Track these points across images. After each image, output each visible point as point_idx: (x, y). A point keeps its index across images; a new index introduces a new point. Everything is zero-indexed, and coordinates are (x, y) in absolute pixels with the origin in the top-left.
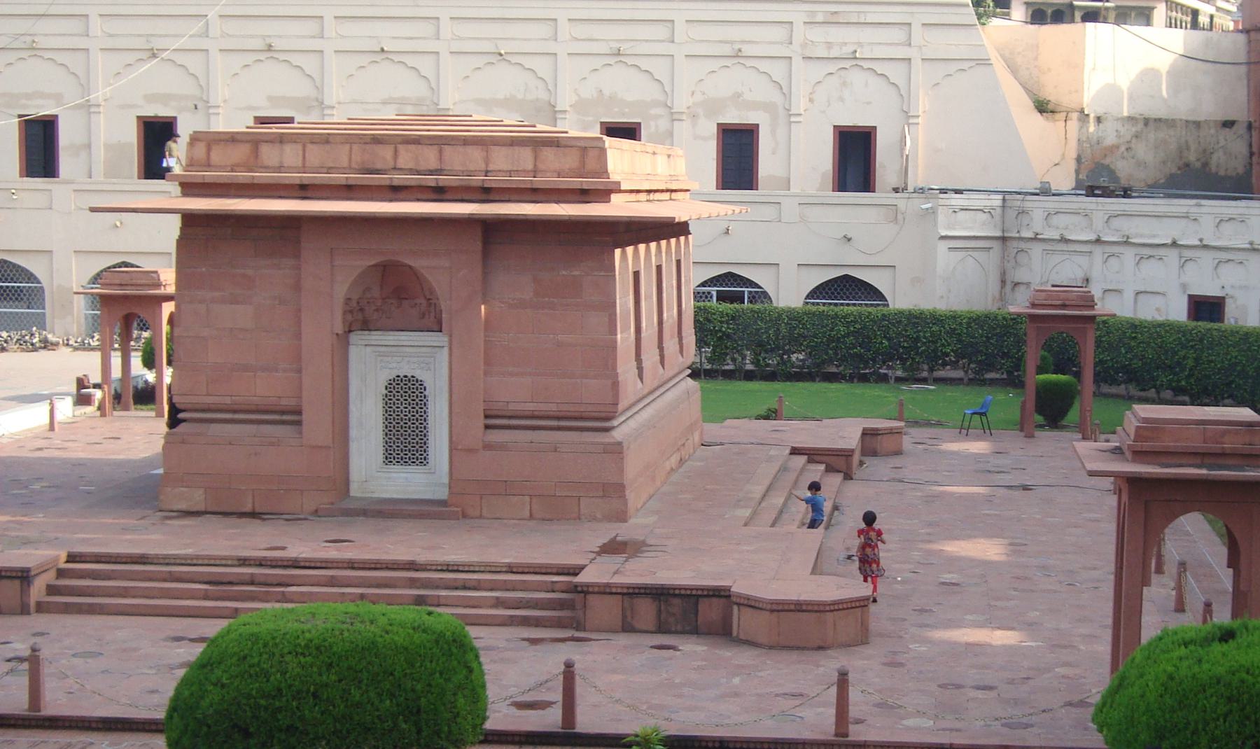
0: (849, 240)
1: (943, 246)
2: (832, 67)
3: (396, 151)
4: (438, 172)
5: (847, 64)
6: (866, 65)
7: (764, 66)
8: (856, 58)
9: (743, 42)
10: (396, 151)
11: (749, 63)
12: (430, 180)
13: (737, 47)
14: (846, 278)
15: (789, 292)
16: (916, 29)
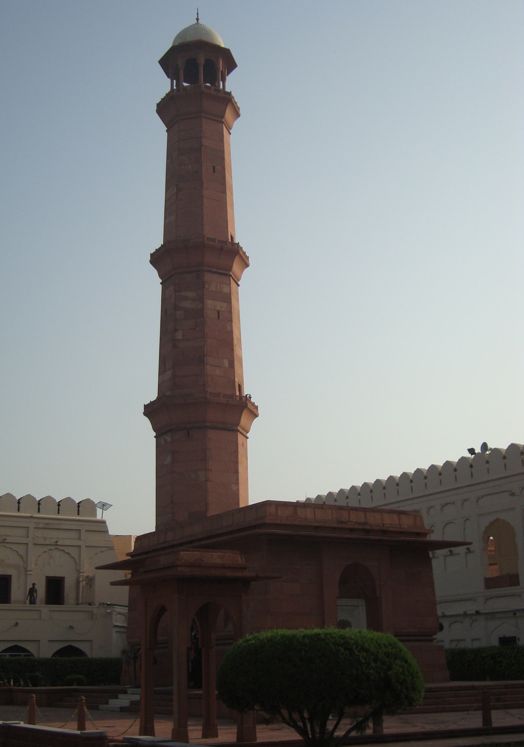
0: (73, 628)
1: (114, 630)
2: (46, 549)
3: (349, 514)
4: (365, 524)
5: (53, 548)
6: (61, 548)
7: (15, 547)
8: (57, 545)
9: (6, 536)
10: (349, 514)
11: (8, 546)
12: (368, 527)
13: (4, 538)
14: (70, 647)
15: (46, 652)
16: (83, 532)
